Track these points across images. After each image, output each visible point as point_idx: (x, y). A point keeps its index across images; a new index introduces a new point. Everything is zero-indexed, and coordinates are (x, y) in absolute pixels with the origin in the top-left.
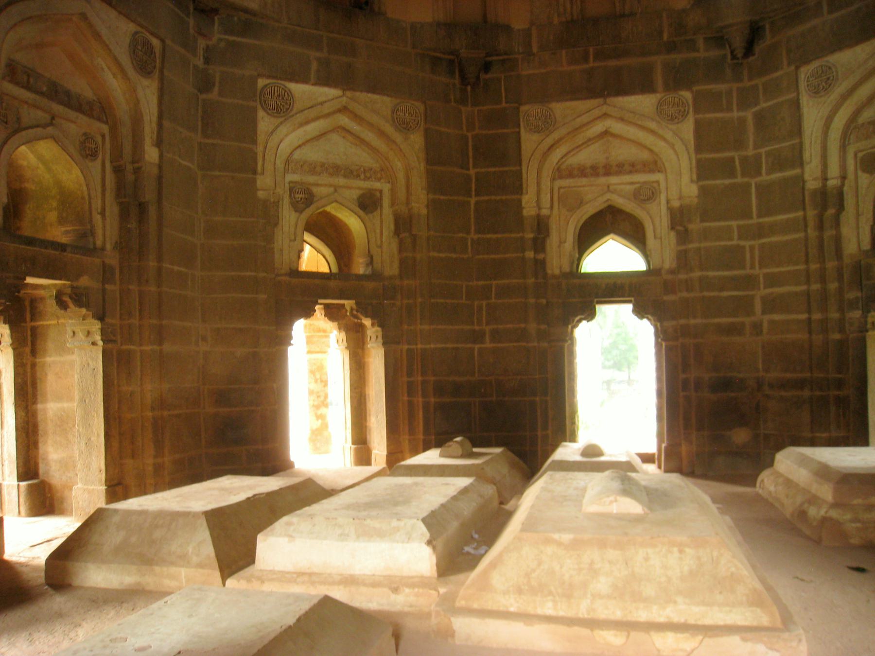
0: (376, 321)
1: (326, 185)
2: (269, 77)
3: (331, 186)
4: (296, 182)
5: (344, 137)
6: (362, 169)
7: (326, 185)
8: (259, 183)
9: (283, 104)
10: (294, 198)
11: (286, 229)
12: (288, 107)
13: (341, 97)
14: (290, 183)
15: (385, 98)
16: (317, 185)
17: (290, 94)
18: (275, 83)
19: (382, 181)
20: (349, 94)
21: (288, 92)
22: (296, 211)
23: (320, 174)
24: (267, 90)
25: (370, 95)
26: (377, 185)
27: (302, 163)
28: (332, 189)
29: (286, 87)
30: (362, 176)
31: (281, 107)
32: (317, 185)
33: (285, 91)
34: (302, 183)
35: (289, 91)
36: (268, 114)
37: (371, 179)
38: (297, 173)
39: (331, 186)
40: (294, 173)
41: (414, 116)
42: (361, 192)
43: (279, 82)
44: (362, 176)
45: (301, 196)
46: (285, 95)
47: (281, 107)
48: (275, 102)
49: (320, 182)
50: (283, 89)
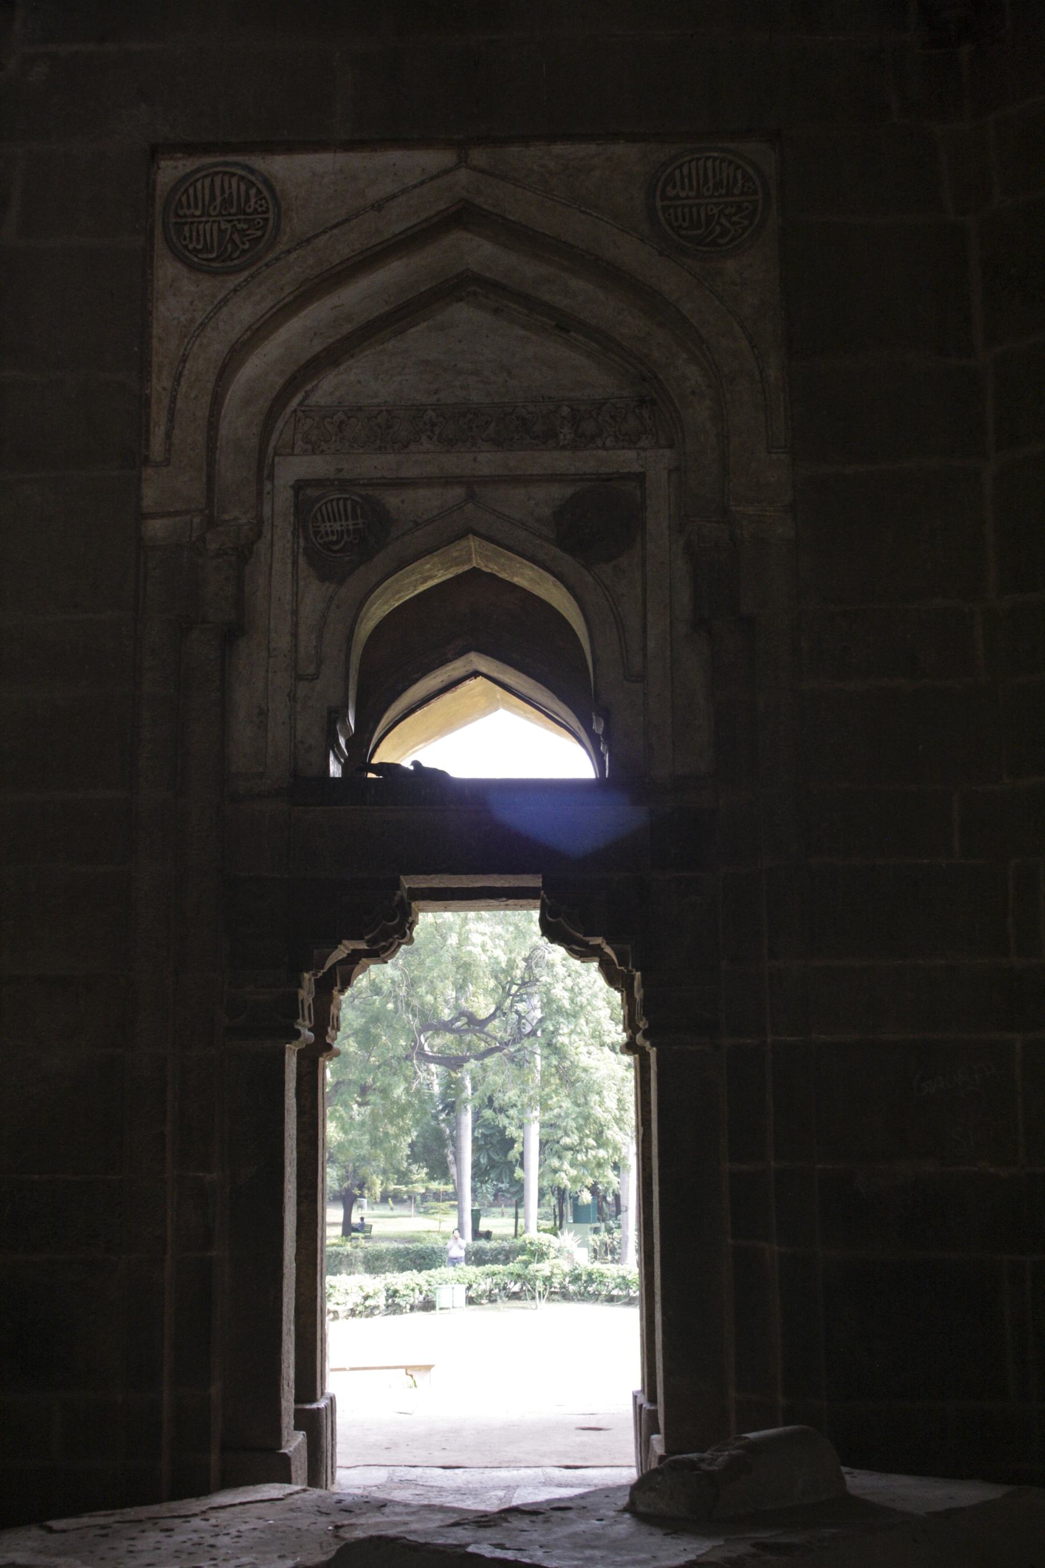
0: (628, 947)
1: (429, 482)
2: (190, 149)
3: (447, 481)
4: (319, 483)
5: (496, 311)
6: (565, 410)
7: (429, 482)
8: (150, 495)
9: (239, 226)
10: (316, 533)
11: (282, 642)
12: (259, 233)
13: (446, 172)
14: (299, 486)
15: (620, 149)
16: (400, 484)
17: (266, 193)
18: (215, 165)
19: (643, 443)
20: (479, 156)
21: (260, 186)
22: (323, 578)
23: (406, 446)
24: (186, 190)
25: (558, 148)
26: (626, 459)
27: (341, 415)
28: (457, 492)
29: (252, 171)
30: (566, 434)
31: (236, 236)
32: (400, 484)
33: (253, 184)
34: (344, 484)
35: (266, 181)
36: (192, 267)
37: (599, 443)
38: (323, 451)
39: (447, 481)
40: (314, 453)
41: (736, 191)
42: (569, 491)
43: (231, 158)
44: (566, 434)
45: (337, 526)
46: (248, 195)
47: (236, 236)
48: (215, 226)
49: (410, 471)
50: (242, 178)
